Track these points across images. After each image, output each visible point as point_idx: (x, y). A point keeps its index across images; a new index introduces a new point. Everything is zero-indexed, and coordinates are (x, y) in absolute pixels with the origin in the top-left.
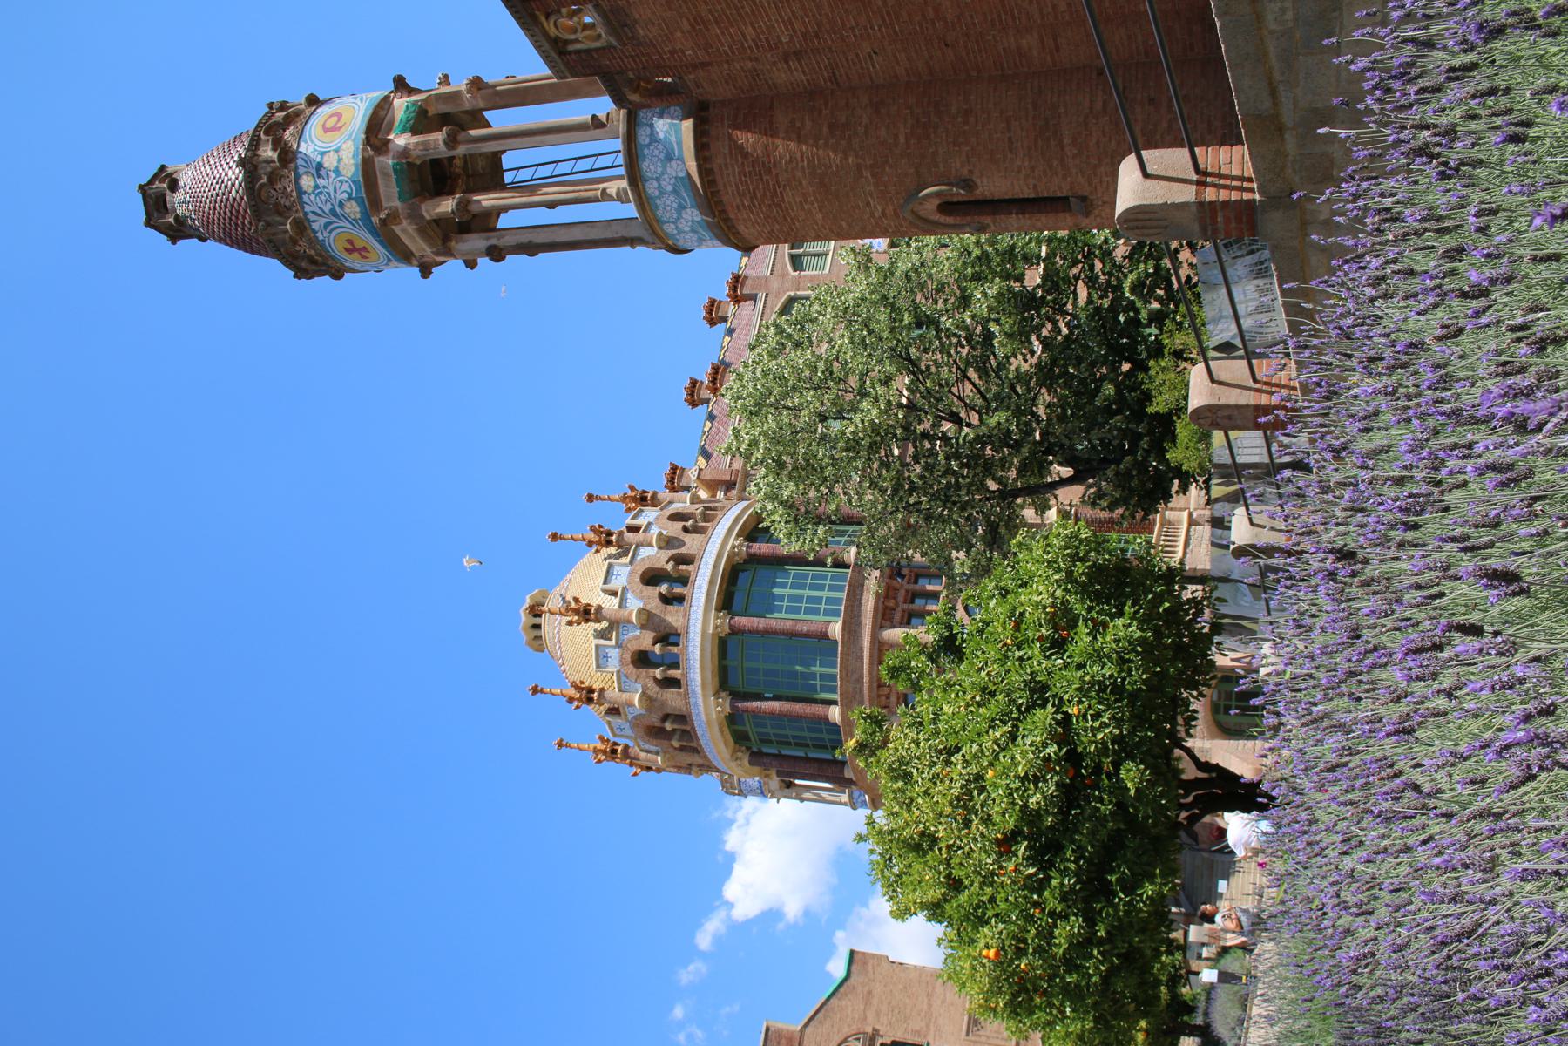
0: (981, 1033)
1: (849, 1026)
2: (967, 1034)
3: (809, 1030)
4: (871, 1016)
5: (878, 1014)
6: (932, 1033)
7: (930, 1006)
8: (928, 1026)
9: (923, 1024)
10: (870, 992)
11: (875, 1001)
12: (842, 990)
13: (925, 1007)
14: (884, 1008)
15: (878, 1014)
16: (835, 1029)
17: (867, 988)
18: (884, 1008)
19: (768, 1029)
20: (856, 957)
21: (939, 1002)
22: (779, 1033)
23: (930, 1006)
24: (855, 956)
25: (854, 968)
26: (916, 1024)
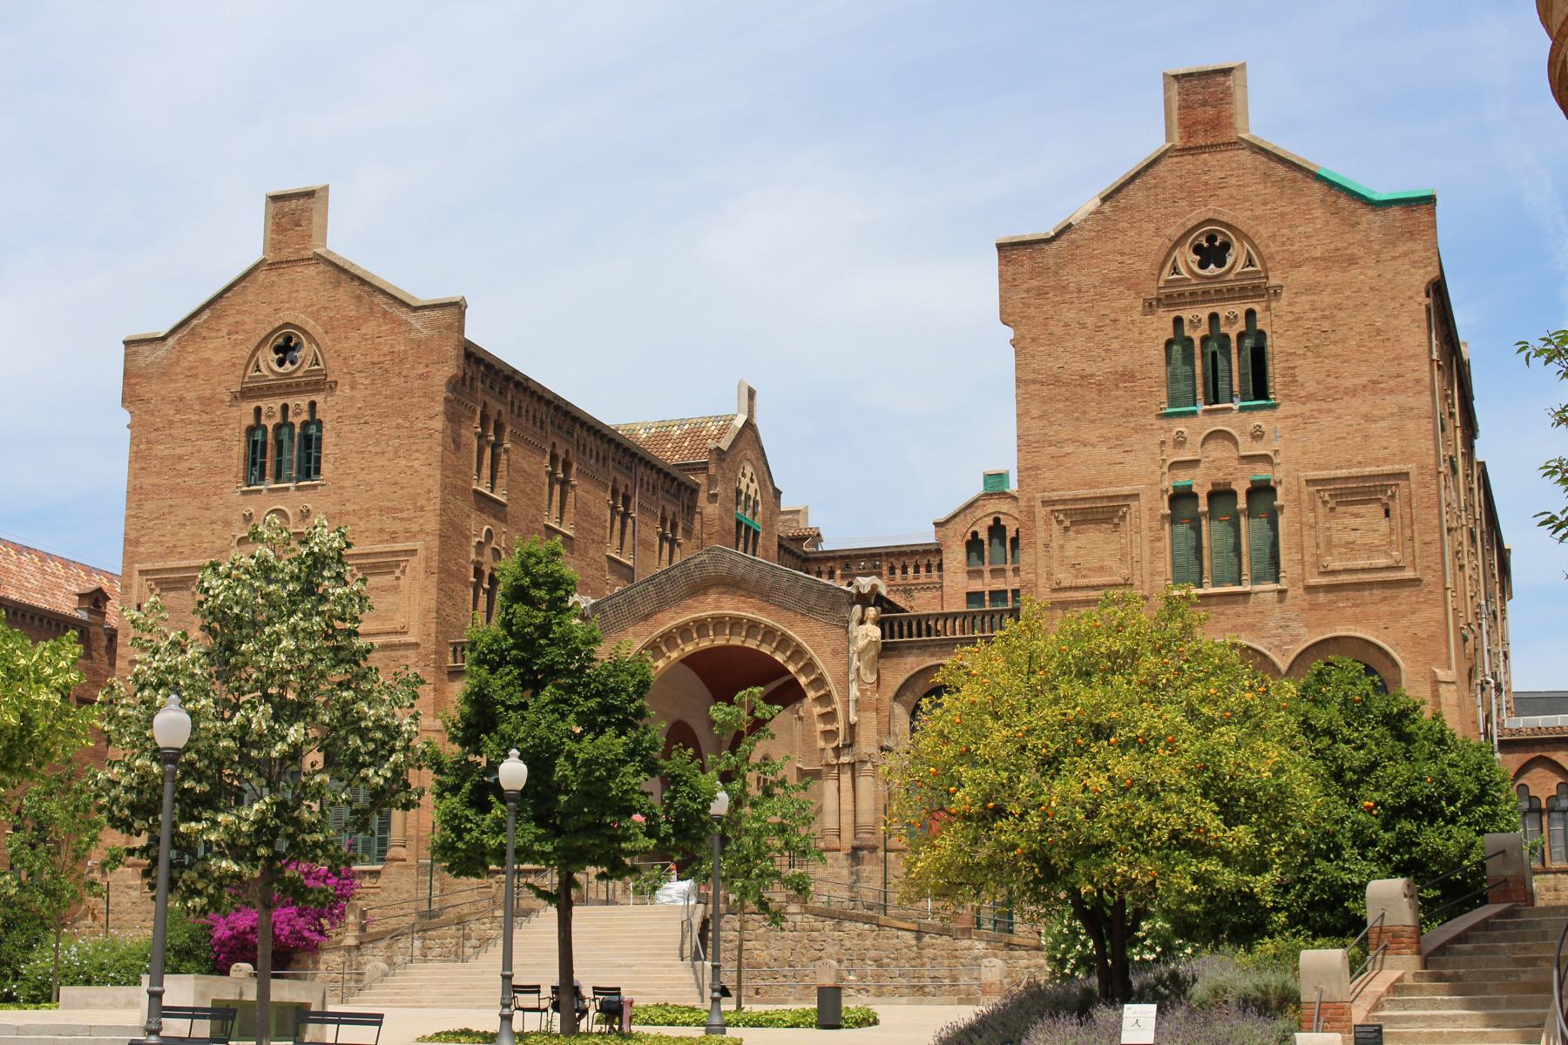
0: (1321, 509)
1: (1273, 237)
2: (1309, 482)
3: (1245, 156)
4: (1305, 274)
5: (1312, 289)
6: (1299, 409)
7: (1354, 392)
8: (1310, 397)
9: (1311, 387)
10: (1352, 261)
11: (1336, 276)
12: (1343, 202)
13: (1349, 383)
14: (1326, 299)
15: (1312, 289)
16: (1259, 211)
17: (1358, 251)
18: (1326, 299)
19: (1226, 72)
20: (1421, 215)
21: (1364, 409)
22: (1221, 100)
23: (1354, 392)
24: (1424, 208)
25: (1396, 212)
26: (1309, 375)
